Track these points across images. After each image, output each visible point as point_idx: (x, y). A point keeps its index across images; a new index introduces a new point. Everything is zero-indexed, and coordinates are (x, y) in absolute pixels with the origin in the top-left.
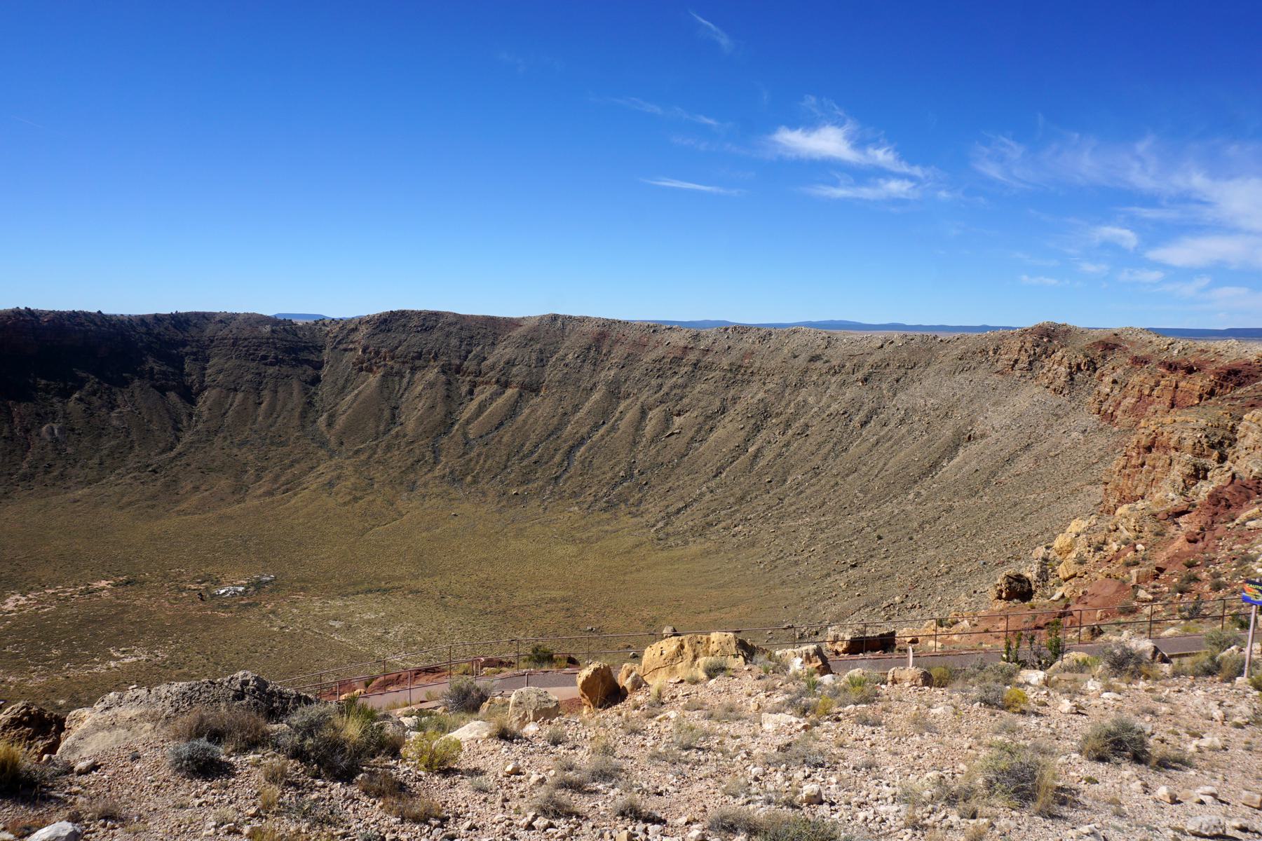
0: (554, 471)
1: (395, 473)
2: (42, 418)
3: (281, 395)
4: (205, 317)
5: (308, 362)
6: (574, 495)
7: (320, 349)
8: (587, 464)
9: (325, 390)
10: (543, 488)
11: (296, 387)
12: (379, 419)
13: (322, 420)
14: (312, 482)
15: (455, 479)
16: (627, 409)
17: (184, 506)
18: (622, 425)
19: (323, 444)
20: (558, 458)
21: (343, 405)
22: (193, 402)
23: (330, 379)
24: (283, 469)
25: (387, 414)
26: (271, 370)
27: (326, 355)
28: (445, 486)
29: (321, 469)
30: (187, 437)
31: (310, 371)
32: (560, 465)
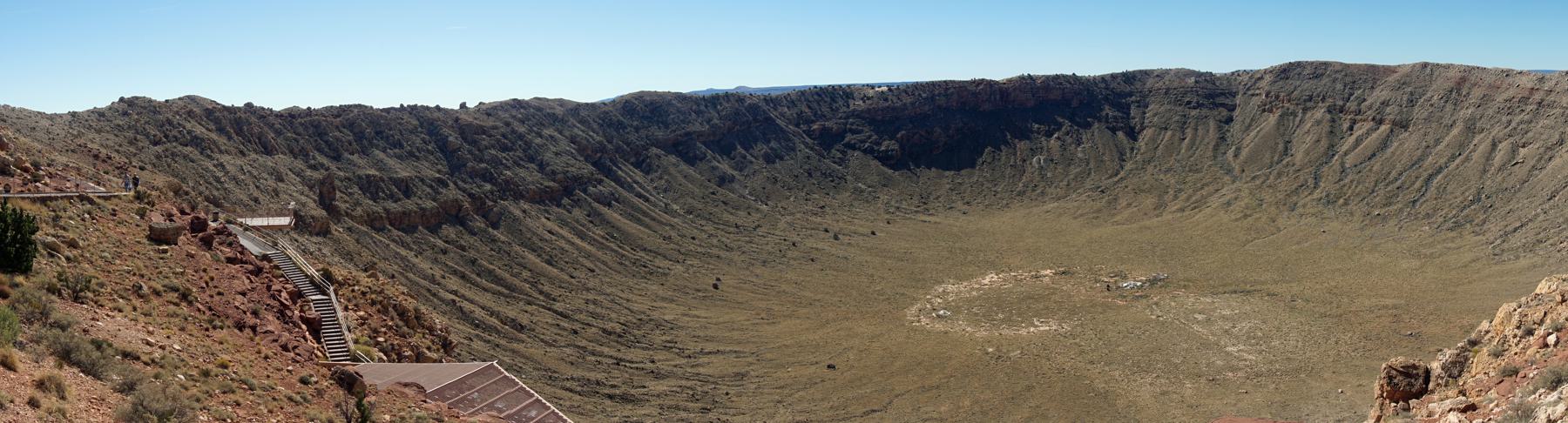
0: (1412, 197)
1: (1281, 196)
2: (1033, 152)
3: (1200, 132)
4: (1146, 73)
5: (1223, 105)
6: (1428, 216)
7: (1234, 95)
8: (1442, 190)
9: (1236, 127)
10: (1401, 210)
11: (1212, 124)
12: (1274, 151)
13: (1231, 153)
14: (1215, 202)
15: (1329, 201)
16: (1480, 142)
17: (1118, 218)
18: (1475, 156)
19: (1229, 172)
20: (1418, 185)
21: (1247, 140)
22: (1135, 140)
23: (1240, 119)
24: (1195, 191)
25: (1281, 147)
26: (1193, 113)
27: (1238, 100)
28: (1321, 207)
29: (1224, 191)
30: (1128, 166)
31: (1225, 113)
32: (1419, 190)
